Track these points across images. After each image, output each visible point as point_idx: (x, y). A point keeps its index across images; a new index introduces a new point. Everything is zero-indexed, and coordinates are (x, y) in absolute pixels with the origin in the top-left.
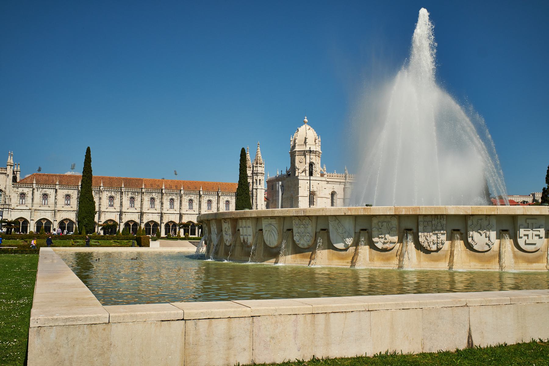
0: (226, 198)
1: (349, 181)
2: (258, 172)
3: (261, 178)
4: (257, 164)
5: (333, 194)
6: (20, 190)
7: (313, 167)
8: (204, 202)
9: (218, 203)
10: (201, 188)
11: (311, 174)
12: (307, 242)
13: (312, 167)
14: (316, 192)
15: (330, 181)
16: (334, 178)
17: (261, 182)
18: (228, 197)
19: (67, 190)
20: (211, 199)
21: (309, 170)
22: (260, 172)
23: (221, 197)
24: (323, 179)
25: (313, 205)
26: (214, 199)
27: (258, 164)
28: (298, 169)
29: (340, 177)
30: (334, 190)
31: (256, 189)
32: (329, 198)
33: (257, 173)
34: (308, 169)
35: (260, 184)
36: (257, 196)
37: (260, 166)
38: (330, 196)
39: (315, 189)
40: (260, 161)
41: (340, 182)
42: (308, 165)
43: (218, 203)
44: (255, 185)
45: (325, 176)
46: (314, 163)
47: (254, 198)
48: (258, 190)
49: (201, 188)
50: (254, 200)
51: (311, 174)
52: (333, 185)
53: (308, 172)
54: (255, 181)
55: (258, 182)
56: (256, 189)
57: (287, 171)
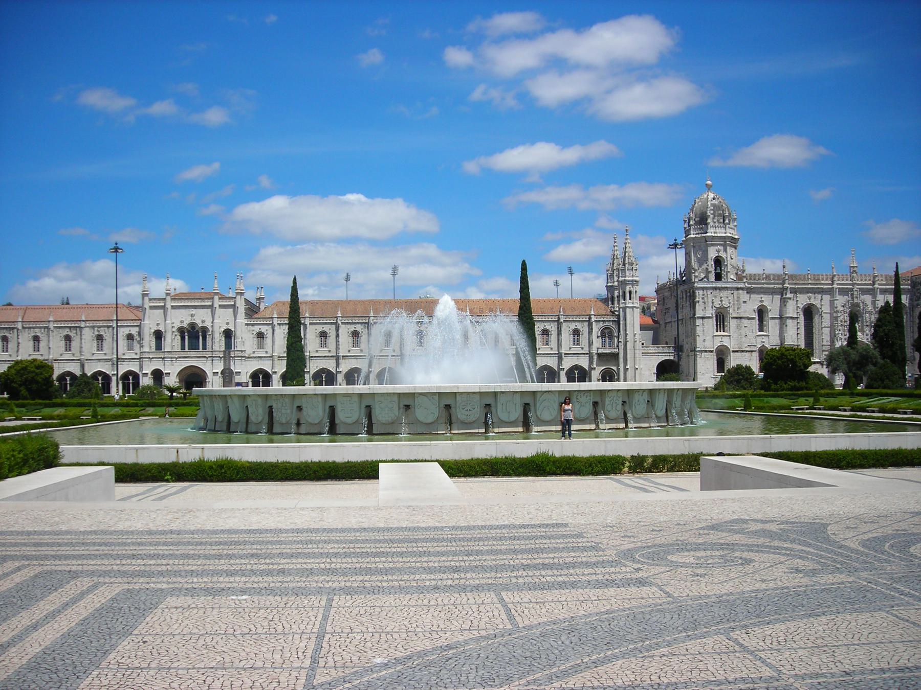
0: (573, 326)
2: (627, 278)
4: (624, 264)
5: (761, 312)
6: (257, 329)
9: (559, 333)
11: (718, 277)
12: (493, 404)
16: (763, 282)
17: (632, 296)
18: (577, 324)
19: (321, 326)
20: (548, 327)
21: (715, 270)
22: (630, 279)
23: (564, 326)
28: (695, 270)
32: (753, 318)
35: (630, 299)
38: (756, 316)
39: (726, 304)
42: (711, 263)
43: (559, 333)
44: (622, 301)
46: (724, 259)
50: (621, 326)
51: (718, 277)
53: (712, 277)
55: (628, 295)
57: (681, 274)
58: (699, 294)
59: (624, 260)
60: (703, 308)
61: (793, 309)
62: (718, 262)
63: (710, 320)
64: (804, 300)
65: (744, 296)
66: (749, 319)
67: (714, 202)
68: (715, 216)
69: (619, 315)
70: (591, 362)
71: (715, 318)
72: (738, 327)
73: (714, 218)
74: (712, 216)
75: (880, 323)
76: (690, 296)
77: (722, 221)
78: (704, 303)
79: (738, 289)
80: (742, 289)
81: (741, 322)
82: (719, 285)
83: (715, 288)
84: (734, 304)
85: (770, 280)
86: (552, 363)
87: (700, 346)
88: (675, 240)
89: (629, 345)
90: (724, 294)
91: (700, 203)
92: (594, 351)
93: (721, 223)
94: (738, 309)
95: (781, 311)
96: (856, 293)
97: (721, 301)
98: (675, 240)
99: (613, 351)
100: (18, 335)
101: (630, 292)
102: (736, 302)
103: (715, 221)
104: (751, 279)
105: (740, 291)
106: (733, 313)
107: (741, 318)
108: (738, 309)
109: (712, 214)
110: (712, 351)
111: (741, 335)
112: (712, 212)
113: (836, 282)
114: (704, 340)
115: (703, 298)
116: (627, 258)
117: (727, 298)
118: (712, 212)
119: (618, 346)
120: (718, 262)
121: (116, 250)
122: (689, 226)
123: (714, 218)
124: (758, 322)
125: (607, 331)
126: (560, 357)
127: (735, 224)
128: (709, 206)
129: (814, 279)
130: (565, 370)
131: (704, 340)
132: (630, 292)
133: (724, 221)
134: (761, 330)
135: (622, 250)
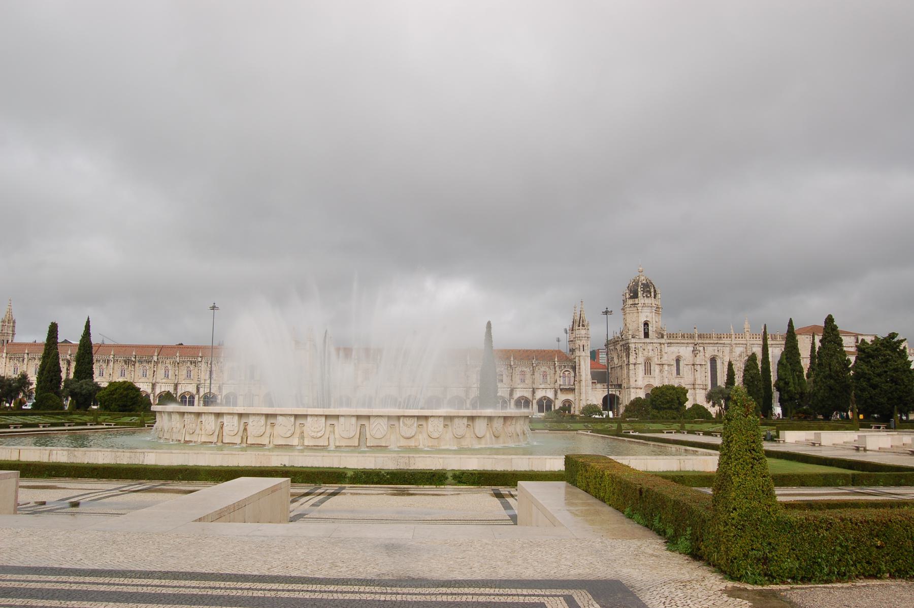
0: (543, 369)
1: (700, 341)
3: (585, 344)
4: (579, 326)
5: (678, 361)
7: (649, 326)
8: (517, 374)
10: (512, 357)
11: (646, 335)
13: (648, 326)
14: (654, 358)
15: (673, 343)
24: (663, 341)
25: (650, 374)
26: (528, 370)
27: (581, 326)
29: (687, 337)
30: (680, 354)
31: (579, 356)
33: (579, 337)
34: (642, 329)
36: (580, 365)
37: (584, 328)
39: (651, 354)
40: (583, 322)
41: (687, 343)
45: (665, 337)
47: (577, 367)
48: (581, 357)
49: (512, 357)
50: (577, 370)
51: (646, 335)
52: (678, 348)
54: (577, 346)
56: (579, 356)
58: (632, 346)
59: (580, 323)
60: (635, 357)
61: (703, 358)
62: (646, 324)
63: (640, 365)
64: (710, 351)
65: (666, 349)
66: (669, 365)
67: (644, 282)
68: (644, 292)
69: (575, 362)
70: (556, 395)
71: (644, 365)
72: (661, 371)
73: (643, 294)
74: (642, 292)
75: (747, 368)
76: (626, 349)
77: (649, 295)
78: (636, 354)
79: (661, 344)
80: (664, 344)
81: (663, 367)
82: (647, 340)
83: (644, 343)
84: (658, 355)
85: (684, 337)
86: (528, 394)
87: (632, 383)
88: (607, 309)
89: (583, 383)
90: (650, 347)
91: (634, 283)
92: (557, 386)
93: (648, 297)
94: (661, 358)
95: (694, 360)
96: (748, 347)
97: (649, 352)
98: (607, 309)
99: (571, 387)
100: (154, 366)
101: (583, 346)
102: (659, 354)
103: (644, 295)
104: (670, 337)
105: (663, 346)
106: (655, 360)
107: (663, 364)
108: (661, 358)
109: (642, 291)
110: (641, 388)
111: (663, 377)
112: (642, 289)
113: (733, 339)
114: (636, 381)
115: (635, 351)
116: (581, 322)
117: (653, 350)
118: (642, 289)
119: (574, 384)
120: (646, 324)
121: (213, 308)
122: (626, 299)
123: (643, 294)
124: (676, 368)
125: (567, 373)
126: (534, 392)
127: (659, 297)
128: (640, 284)
129: (718, 337)
130: (536, 400)
131: (636, 381)
132: (583, 346)
133: (651, 295)
134: (678, 373)
135: (579, 316)
